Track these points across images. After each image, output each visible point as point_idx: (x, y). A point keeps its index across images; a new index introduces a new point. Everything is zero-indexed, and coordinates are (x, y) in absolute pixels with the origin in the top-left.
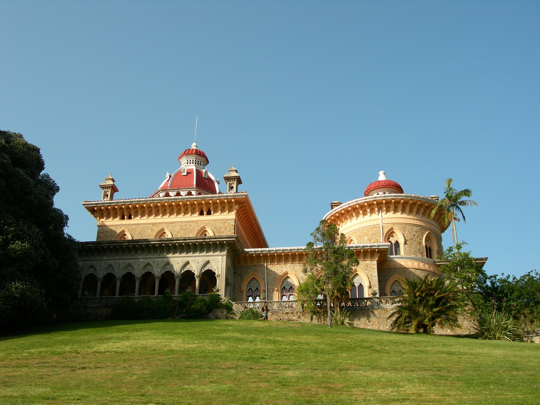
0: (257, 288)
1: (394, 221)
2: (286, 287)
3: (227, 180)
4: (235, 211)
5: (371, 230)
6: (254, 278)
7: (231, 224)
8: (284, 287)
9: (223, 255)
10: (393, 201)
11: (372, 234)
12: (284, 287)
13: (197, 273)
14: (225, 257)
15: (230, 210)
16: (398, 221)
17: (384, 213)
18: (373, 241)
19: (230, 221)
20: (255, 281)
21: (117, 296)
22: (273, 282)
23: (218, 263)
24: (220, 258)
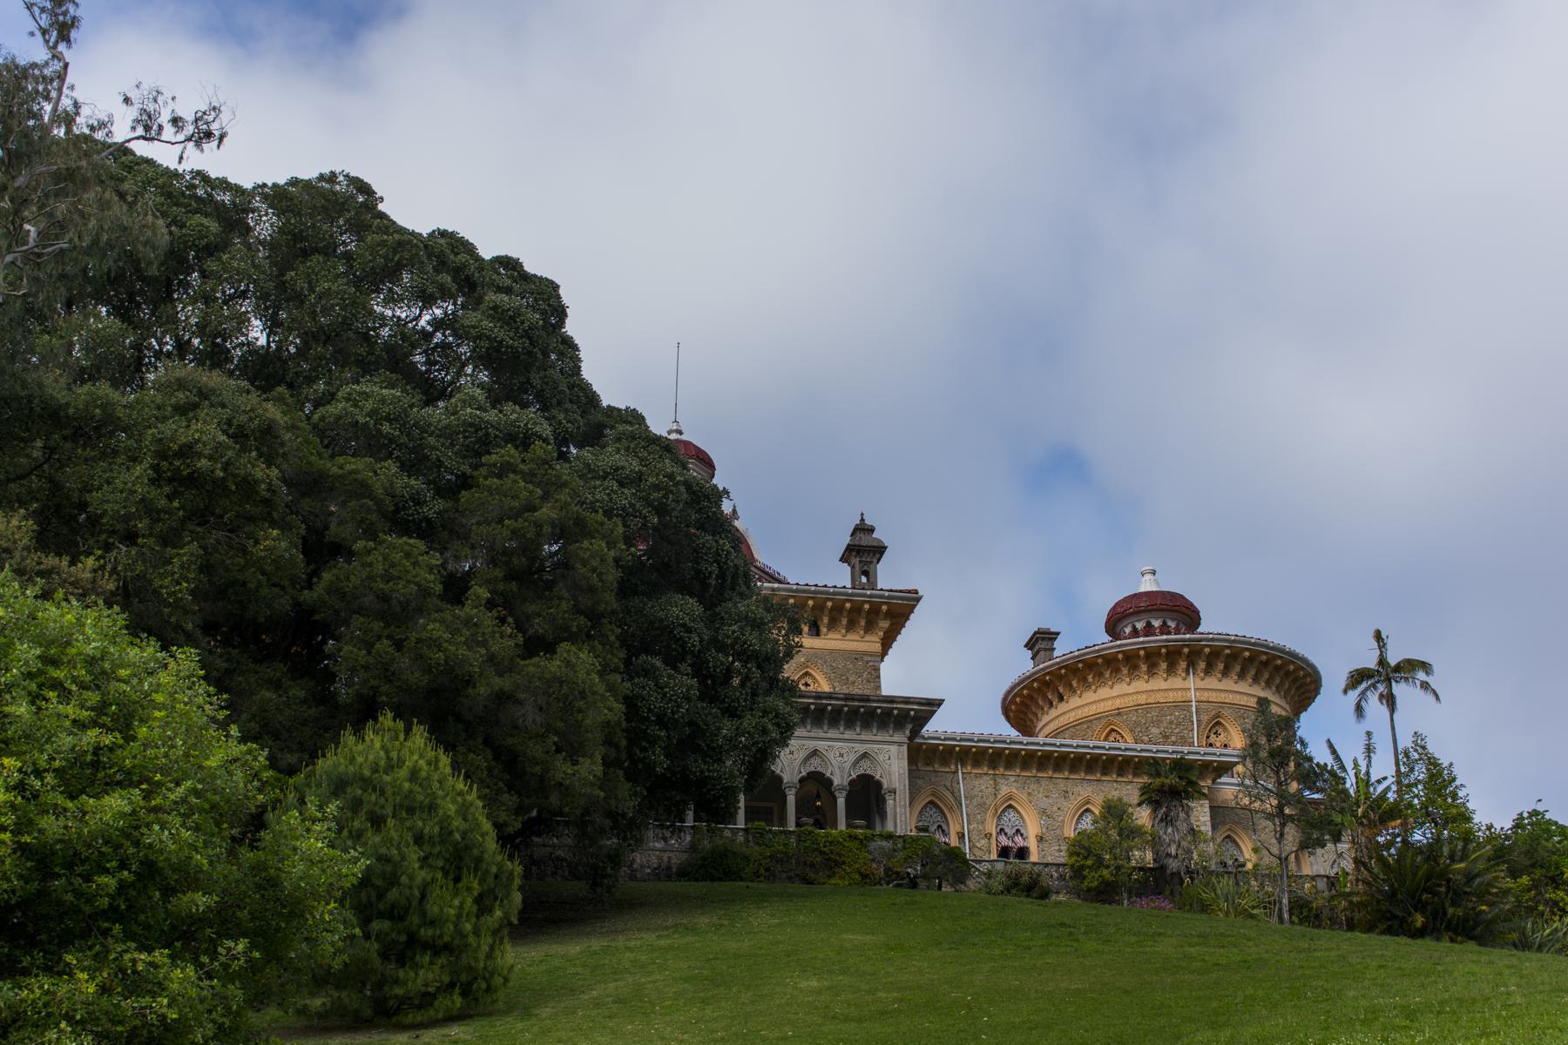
0: (939, 827)
1: (1222, 697)
2: (1007, 830)
3: (854, 553)
4: (881, 634)
5: (1168, 713)
6: (931, 802)
7: (871, 664)
8: (1002, 830)
9: (900, 744)
10: (1228, 651)
11: (1171, 722)
12: (1002, 830)
13: (840, 779)
14: (905, 747)
15: (869, 628)
16: (1230, 698)
17: (1198, 680)
18: (1173, 738)
19: (869, 658)
20: (934, 810)
21: (842, 826)
22: (979, 816)
23: (889, 762)
24: (894, 748)
